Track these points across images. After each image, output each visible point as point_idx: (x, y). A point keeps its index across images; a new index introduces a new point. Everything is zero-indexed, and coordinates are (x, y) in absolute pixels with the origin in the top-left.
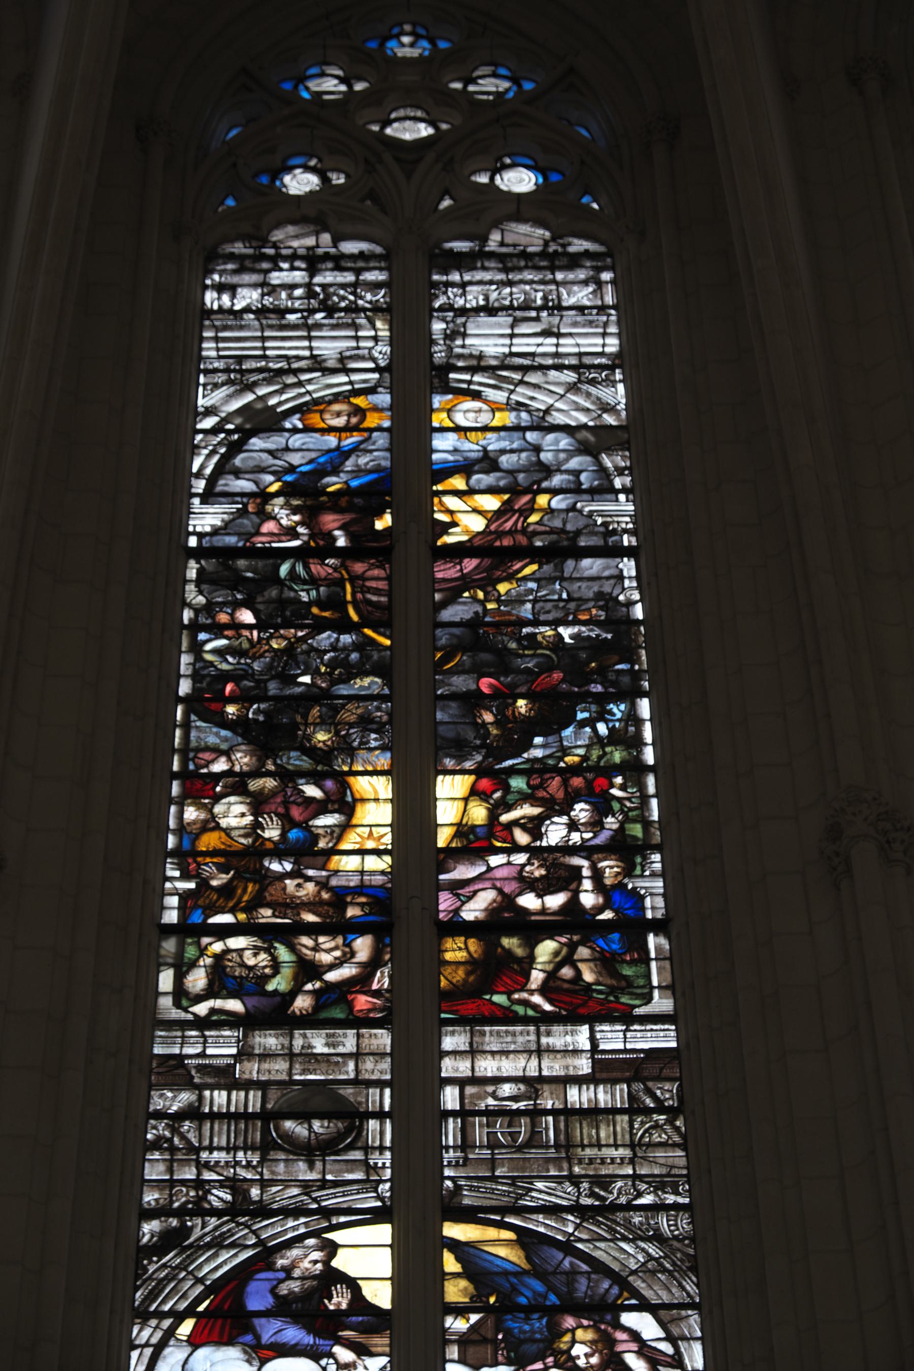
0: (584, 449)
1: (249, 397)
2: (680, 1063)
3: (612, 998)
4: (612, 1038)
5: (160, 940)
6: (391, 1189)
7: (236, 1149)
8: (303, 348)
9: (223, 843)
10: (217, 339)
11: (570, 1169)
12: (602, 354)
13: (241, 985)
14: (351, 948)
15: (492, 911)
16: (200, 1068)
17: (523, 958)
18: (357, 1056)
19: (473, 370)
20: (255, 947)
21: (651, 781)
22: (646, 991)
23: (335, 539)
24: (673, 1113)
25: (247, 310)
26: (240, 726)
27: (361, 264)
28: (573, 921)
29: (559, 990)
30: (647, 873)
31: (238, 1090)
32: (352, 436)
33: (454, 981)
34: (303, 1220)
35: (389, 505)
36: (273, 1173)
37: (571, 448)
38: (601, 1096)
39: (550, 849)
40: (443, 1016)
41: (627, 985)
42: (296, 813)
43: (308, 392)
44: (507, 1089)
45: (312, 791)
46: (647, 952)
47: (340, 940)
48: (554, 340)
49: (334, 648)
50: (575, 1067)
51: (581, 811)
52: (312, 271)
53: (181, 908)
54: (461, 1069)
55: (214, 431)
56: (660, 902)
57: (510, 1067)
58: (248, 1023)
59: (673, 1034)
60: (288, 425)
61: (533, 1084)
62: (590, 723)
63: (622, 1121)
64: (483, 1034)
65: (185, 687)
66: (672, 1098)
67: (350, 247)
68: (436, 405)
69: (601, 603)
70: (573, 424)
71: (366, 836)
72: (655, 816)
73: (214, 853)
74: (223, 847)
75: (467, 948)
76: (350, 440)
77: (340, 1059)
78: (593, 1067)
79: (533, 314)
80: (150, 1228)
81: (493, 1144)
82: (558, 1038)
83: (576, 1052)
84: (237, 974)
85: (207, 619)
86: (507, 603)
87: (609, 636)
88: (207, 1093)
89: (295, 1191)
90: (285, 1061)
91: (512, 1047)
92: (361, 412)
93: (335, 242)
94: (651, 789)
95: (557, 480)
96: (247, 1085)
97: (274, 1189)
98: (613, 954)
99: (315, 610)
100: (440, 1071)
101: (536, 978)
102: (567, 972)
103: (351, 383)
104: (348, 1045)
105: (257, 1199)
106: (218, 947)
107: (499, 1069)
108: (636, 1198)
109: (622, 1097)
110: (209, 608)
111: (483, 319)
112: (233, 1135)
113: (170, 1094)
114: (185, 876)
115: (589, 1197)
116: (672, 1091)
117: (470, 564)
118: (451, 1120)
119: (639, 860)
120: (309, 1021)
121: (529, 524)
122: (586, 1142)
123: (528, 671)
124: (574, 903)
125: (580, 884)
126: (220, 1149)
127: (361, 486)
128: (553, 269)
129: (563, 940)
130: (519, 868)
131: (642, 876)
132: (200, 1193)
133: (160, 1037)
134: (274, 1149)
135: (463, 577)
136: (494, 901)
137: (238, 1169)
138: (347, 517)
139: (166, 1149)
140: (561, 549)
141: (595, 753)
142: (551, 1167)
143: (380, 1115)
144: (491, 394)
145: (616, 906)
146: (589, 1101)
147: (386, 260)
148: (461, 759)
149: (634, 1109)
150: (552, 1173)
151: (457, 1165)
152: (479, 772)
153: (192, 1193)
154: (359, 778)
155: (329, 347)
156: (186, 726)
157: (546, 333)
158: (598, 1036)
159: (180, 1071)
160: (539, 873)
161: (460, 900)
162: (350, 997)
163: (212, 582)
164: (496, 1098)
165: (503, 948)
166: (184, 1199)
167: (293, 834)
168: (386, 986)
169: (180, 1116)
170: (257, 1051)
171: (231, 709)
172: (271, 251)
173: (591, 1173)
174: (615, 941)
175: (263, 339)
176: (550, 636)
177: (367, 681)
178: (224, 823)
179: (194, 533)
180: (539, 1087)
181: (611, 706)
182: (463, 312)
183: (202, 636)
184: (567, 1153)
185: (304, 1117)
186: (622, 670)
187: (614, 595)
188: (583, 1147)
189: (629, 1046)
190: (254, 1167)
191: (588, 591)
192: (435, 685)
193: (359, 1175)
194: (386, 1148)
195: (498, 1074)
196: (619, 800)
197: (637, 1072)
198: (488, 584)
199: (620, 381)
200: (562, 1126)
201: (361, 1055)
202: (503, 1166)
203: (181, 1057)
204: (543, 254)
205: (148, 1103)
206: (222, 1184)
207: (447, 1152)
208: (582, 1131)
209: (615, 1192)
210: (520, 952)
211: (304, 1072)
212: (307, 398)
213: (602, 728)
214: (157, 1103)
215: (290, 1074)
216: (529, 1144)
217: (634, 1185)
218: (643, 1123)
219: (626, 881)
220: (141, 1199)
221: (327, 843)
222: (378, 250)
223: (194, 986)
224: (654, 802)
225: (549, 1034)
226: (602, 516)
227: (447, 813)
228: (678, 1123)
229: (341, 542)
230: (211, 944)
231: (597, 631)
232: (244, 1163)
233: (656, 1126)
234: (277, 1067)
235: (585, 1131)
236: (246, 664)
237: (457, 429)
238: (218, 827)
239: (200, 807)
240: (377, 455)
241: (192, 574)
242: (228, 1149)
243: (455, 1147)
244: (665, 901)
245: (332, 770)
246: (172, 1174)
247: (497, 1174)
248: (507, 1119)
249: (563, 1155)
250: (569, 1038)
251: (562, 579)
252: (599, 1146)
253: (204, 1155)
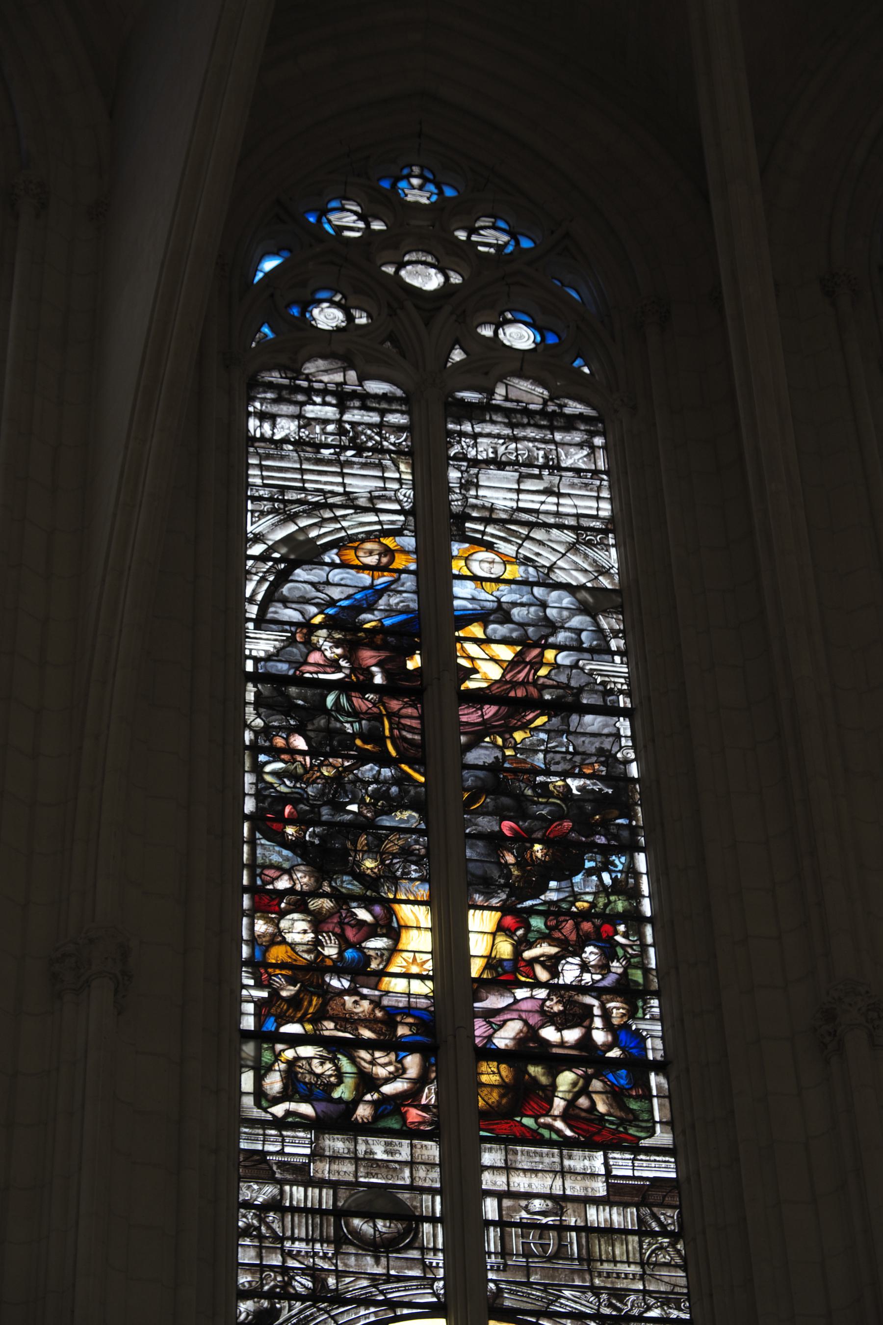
0: (583, 609)
1: (292, 528)
2: (679, 1193)
3: (621, 1129)
4: (623, 1166)
5: (241, 1044)
6: (445, 1287)
7: (314, 1241)
8: (337, 484)
9: (289, 957)
10: (261, 467)
11: (592, 1280)
12: (596, 517)
13: (310, 1090)
14: (402, 1065)
15: (520, 1040)
16: (280, 1164)
17: (547, 1086)
18: (412, 1164)
19: (487, 521)
20: (321, 1057)
21: (649, 930)
22: (650, 1125)
23: (372, 675)
24: (674, 1237)
25: (285, 440)
26: (297, 846)
27: (384, 406)
28: (587, 1055)
29: (577, 1118)
30: (648, 1016)
31: (313, 1187)
32: (383, 576)
33: (490, 1102)
34: (372, 1309)
35: (418, 647)
36: (346, 1265)
37: (573, 607)
38: (615, 1217)
39: (566, 987)
40: (482, 1133)
41: (633, 1118)
42: (350, 933)
43: (343, 528)
44: (537, 1205)
45: (363, 915)
46: (650, 1089)
47: (393, 1056)
48: (554, 500)
49: (376, 780)
50: (593, 1189)
51: (591, 954)
52: (342, 408)
53: (257, 1015)
54: (498, 1183)
55: (263, 558)
56: (659, 1044)
57: (540, 1184)
58: (319, 1126)
59: (673, 1165)
60: (327, 559)
61: (560, 1201)
62: (596, 871)
63: (633, 1241)
64: (515, 1153)
65: (249, 806)
66: (673, 1224)
67: (375, 387)
68: (455, 553)
69: (602, 759)
70: (574, 583)
71: (411, 961)
72: (653, 965)
73: (282, 965)
74: (289, 960)
75: (499, 1073)
76: (383, 579)
77: (397, 1166)
78: (608, 1190)
79: (536, 471)
81: (527, 1254)
82: (578, 1161)
83: (593, 1175)
84: (307, 1080)
85: (265, 741)
86: (523, 751)
87: (610, 791)
88: (287, 1188)
89: (365, 1283)
90: (352, 1164)
91: (540, 1167)
92: (388, 552)
94: (649, 939)
95: (562, 637)
96: (321, 1183)
97: (348, 1280)
98: (622, 1088)
99: (358, 742)
100: (481, 1183)
101: (558, 1106)
102: (583, 1102)
103: (380, 523)
104: (403, 1153)
105: (333, 1287)
106: (289, 1054)
107: (530, 1185)
108: (645, 1311)
109: (632, 1220)
110: (266, 731)
111: (494, 472)
112: (310, 1228)
113: (256, 1187)
114: (259, 985)
115: (608, 1307)
116: (673, 1217)
117: (490, 711)
118: (492, 1229)
119: (640, 1004)
120: (369, 1129)
121: (539, 677)
122: (604, 1257)
123: (542, 818)
124: (587, 1038)
125: (592, 1021)
126: (300, 1240)
127: (393, 626)
128: (552, 429)
129: (580, 1072)
130: (541, 1002)
131: (643, 1019)
132: (286, 1278)
133: (245, 1133)
134: (346, 1244)
135: (484, 722)
136: (521, 1031)
137: (316, 1260)
138: (383, 655)
139: (255, 1236)
140: (567, 705)
141: (602, 901)
142: (576, 1278)
143: (433, 1220)
144: (502, 547)
145: (623, 1045)
146: (605, 1221)
147: (407, 403)
148: (489, 895)
149: (643, 1231)
150: (576, 1283)
151: (498, 1270)
152: (505, 909)
153: (279, 1278)
154: (403, 906)
155: (361, 485)
156: (253, 843)
157: (548, 492)
158: (611, 1162)
159: (264, 1166)
160: (558, 1008)
161: (492, 1027)
162: (404, 1110)
163: (269, 707)
164: (528, 1212)
165: (529, 1075)
166: (272, 1283)
167: (349, 954)
168: (433, 1101)
169: (265, 1208)
170: (327, 1153)
171: (290, 830)
172: (305, 384)
173: (609, 1286)
174: (622, 1077)
176: (560, 787)
177: (406, 814)
178: (289, 938)
179: (250, 657)
180: (563, 1204)
181: (614, 857)
182: (475, 462)
183: (262, 758)
184: (589, 1265)
185: (370, 1216)
186: (622, 825)
187: (613, 752)
188: (602, 1262)
189: (637, 1174)
190: (330, 1259)
191: (591, 745)
192: (465, 824)
193: (417, 1273)
194: (439, 1250)
195: (530, 1190)
196: (623, 946)
197: (644, 1198)
198: (507, 731)
199: (613, 546)
200: (584, 1241)
201: (413, 1162)
202: (536, 1274)
203: (263, 1153)
204: (543, 413)
205: (238, 1193)
206: (304, 1272)
207: (490, 1257)
208: (600, 1248)
209: (629, 1304)
210: (544, 1080)
211: (367, 1175)
212: (343, 534)
213: (606, 878)
214: (246, 1194)
215: (356, 1176)
216: (556, 1256)
217: (644, 1299)
218: (650, 1244)
219: (630, 1022)
220: (237, 1280)
221: (378, 965)
222: (399, 393)
223: (271, 1089)
224: (652, 951)
225: (570, 1157)
226: (601, 675)
227: (478, 945)
228: (679, 1247)
229: (378, 679)
230: (284, 1050)
231: (600, 786)
232: (321, 1254)
233: (661, 1248)
234: (345, 1170)
235: (603, 1247)
236: (301, 788)
237: (474, 578)
238: (284, 941)
239: (269, 921)
240: (404, 597)
241: (250, 697)
242: (307, 1241)
243: (496, 1253)
244: (664, 1043)
245: (374, 892)
246: (261, 1259)
247: (531, 1280)
248: (538, 1232)
249: (585, 1267)
250: (587, 1163)
251: (569, 733)
252: (615, 1262)
253: (288, 1244)
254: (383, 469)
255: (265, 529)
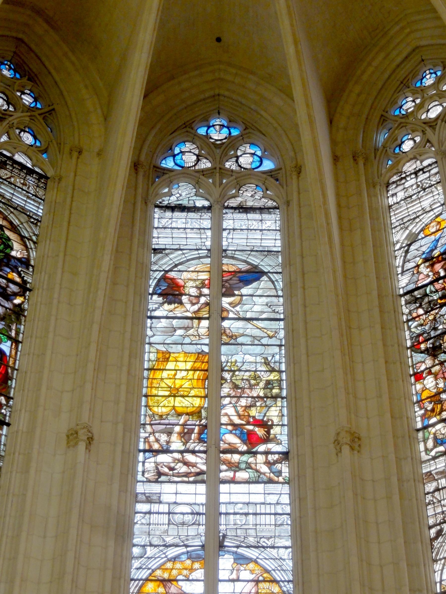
1: (407, 232)
8: (419, 207)
13: (442, 441)
16: (436, 473)
26: (426, 351)
76: (438, 234)
80: (433, 532)
92: (439, 223)
93: (421, 162)
99: (439, 301)
110: (410, 313)
156: (412, 357)
175: (407, 209)
178: (428, 387)
212: (424, 225)
238: (426, 389)
241: (403, 303)
254: (432, 192)
255: (399, 236)
